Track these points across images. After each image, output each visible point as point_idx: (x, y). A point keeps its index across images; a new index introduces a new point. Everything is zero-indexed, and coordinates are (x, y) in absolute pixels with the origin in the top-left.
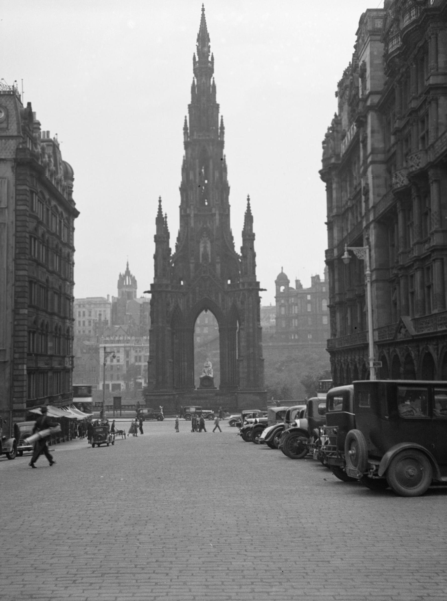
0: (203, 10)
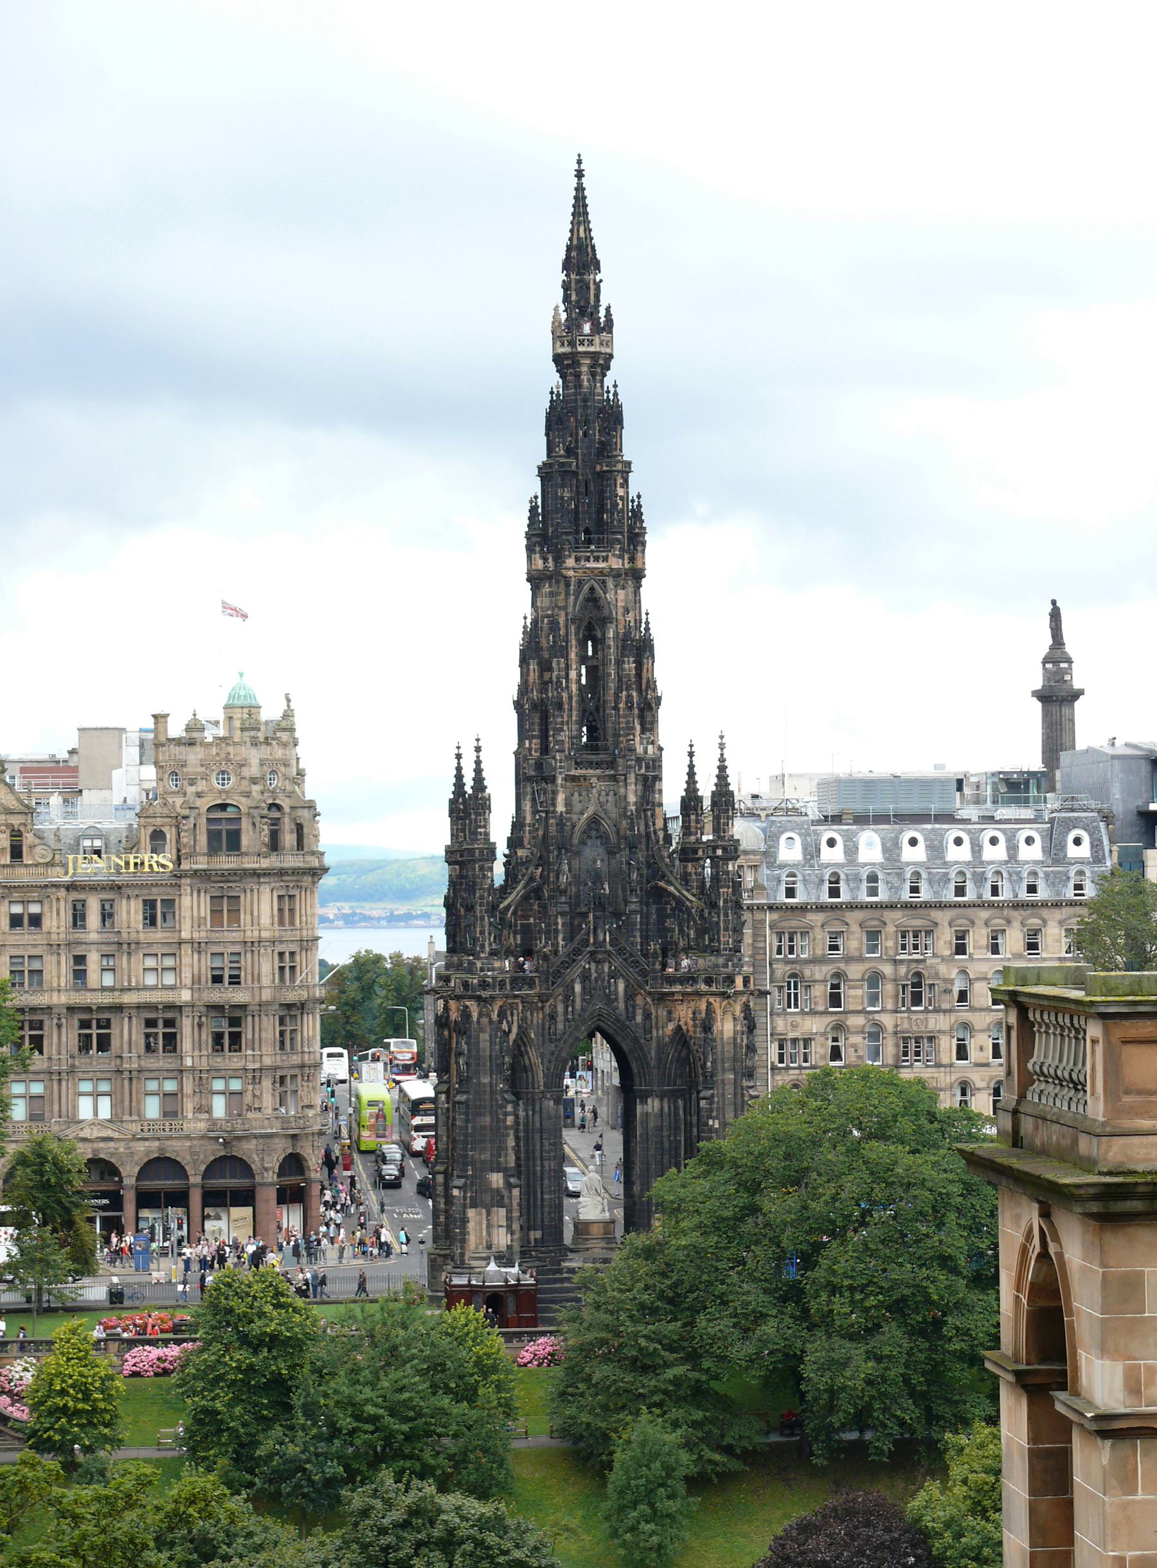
0: (580, 174)
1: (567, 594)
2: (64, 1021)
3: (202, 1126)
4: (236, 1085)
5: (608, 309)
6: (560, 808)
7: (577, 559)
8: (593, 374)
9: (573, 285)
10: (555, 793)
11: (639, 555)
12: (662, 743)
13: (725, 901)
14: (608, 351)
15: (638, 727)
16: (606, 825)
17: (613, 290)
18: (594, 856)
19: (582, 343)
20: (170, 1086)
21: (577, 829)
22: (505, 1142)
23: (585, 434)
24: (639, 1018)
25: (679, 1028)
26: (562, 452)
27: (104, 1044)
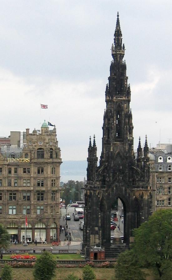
0: (118, 16)
1: (114, 105)
2: (6, 193)
3: (35, 216)
4: (42, 208)
5: (124, 44)
6: (112, 150)
7: (116, 97)
8: (120, 58)
9: (116, 40)
10: (110, 147)
11: (129, 97)
12: (133, 137)
13: (146, 171)
14: (123, 53)
15: (128, 133)
16: (121, 154)
17: (125, 40)
18: (119, 161)
19: (118, 52)
20: (28, 207)
21: (115, 155)
22: (98, 221)
23: (118, 71)
24: (128, 195)
25: (136, 197)
26: (113, 75)
27: (15, 198)
